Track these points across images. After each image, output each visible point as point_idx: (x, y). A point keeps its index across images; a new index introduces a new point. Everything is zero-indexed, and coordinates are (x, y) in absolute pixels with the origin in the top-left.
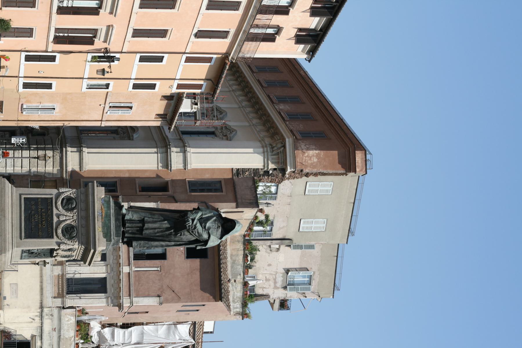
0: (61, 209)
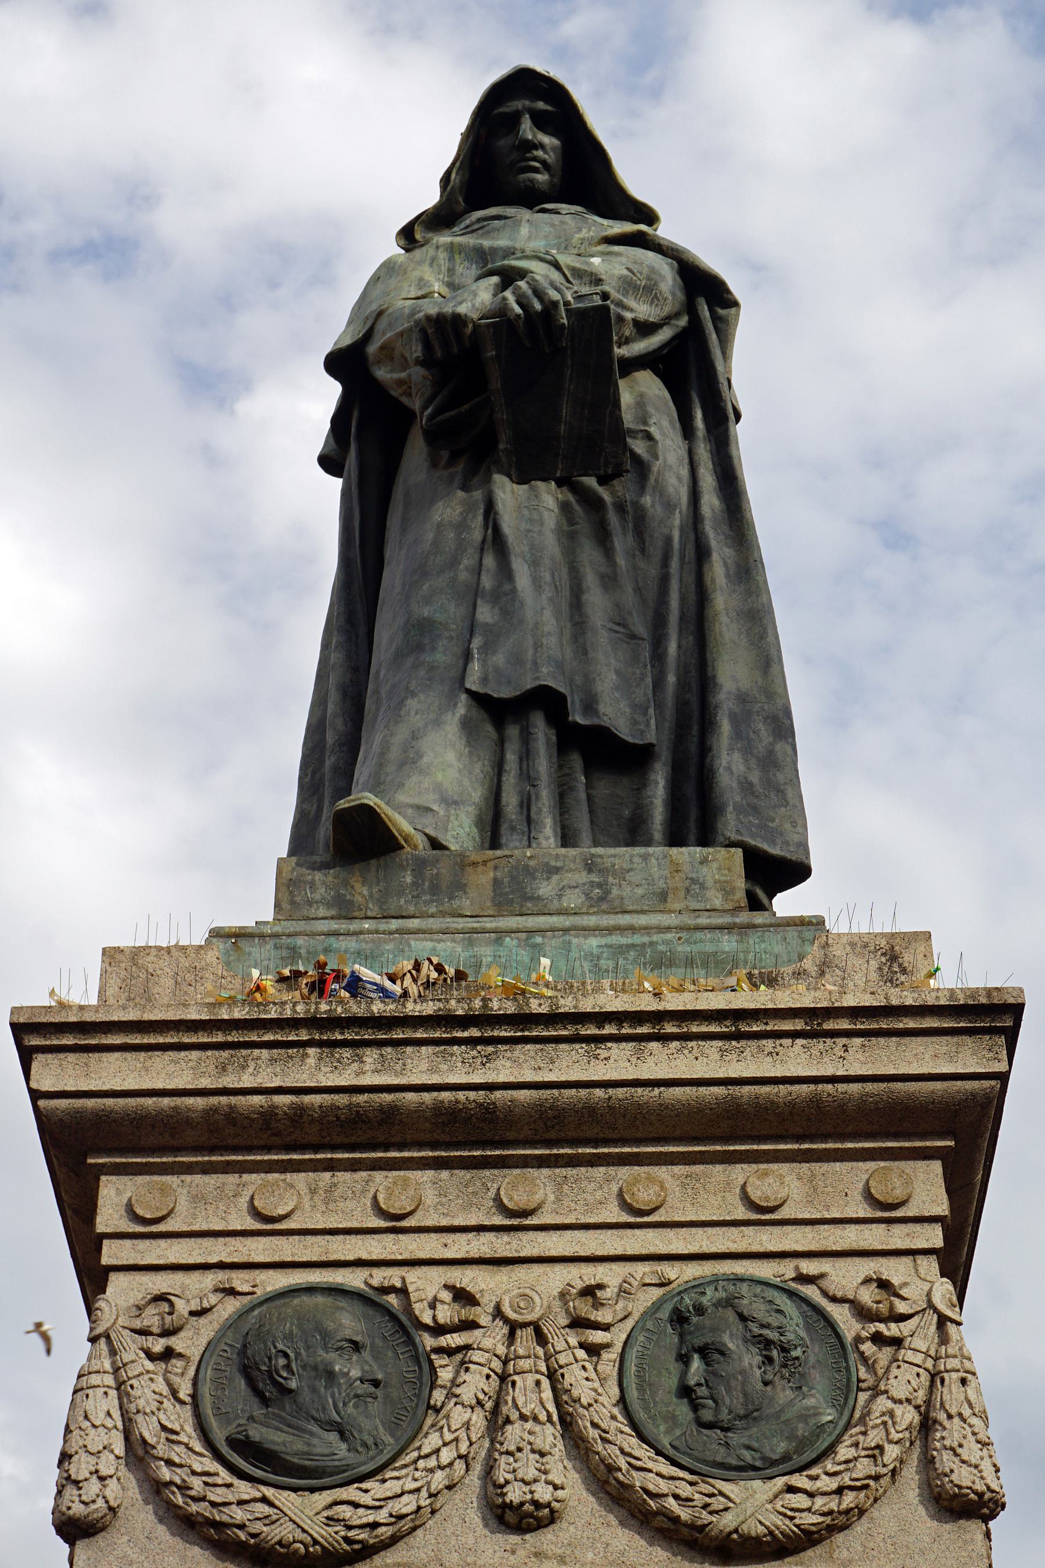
0: (393, 1487)
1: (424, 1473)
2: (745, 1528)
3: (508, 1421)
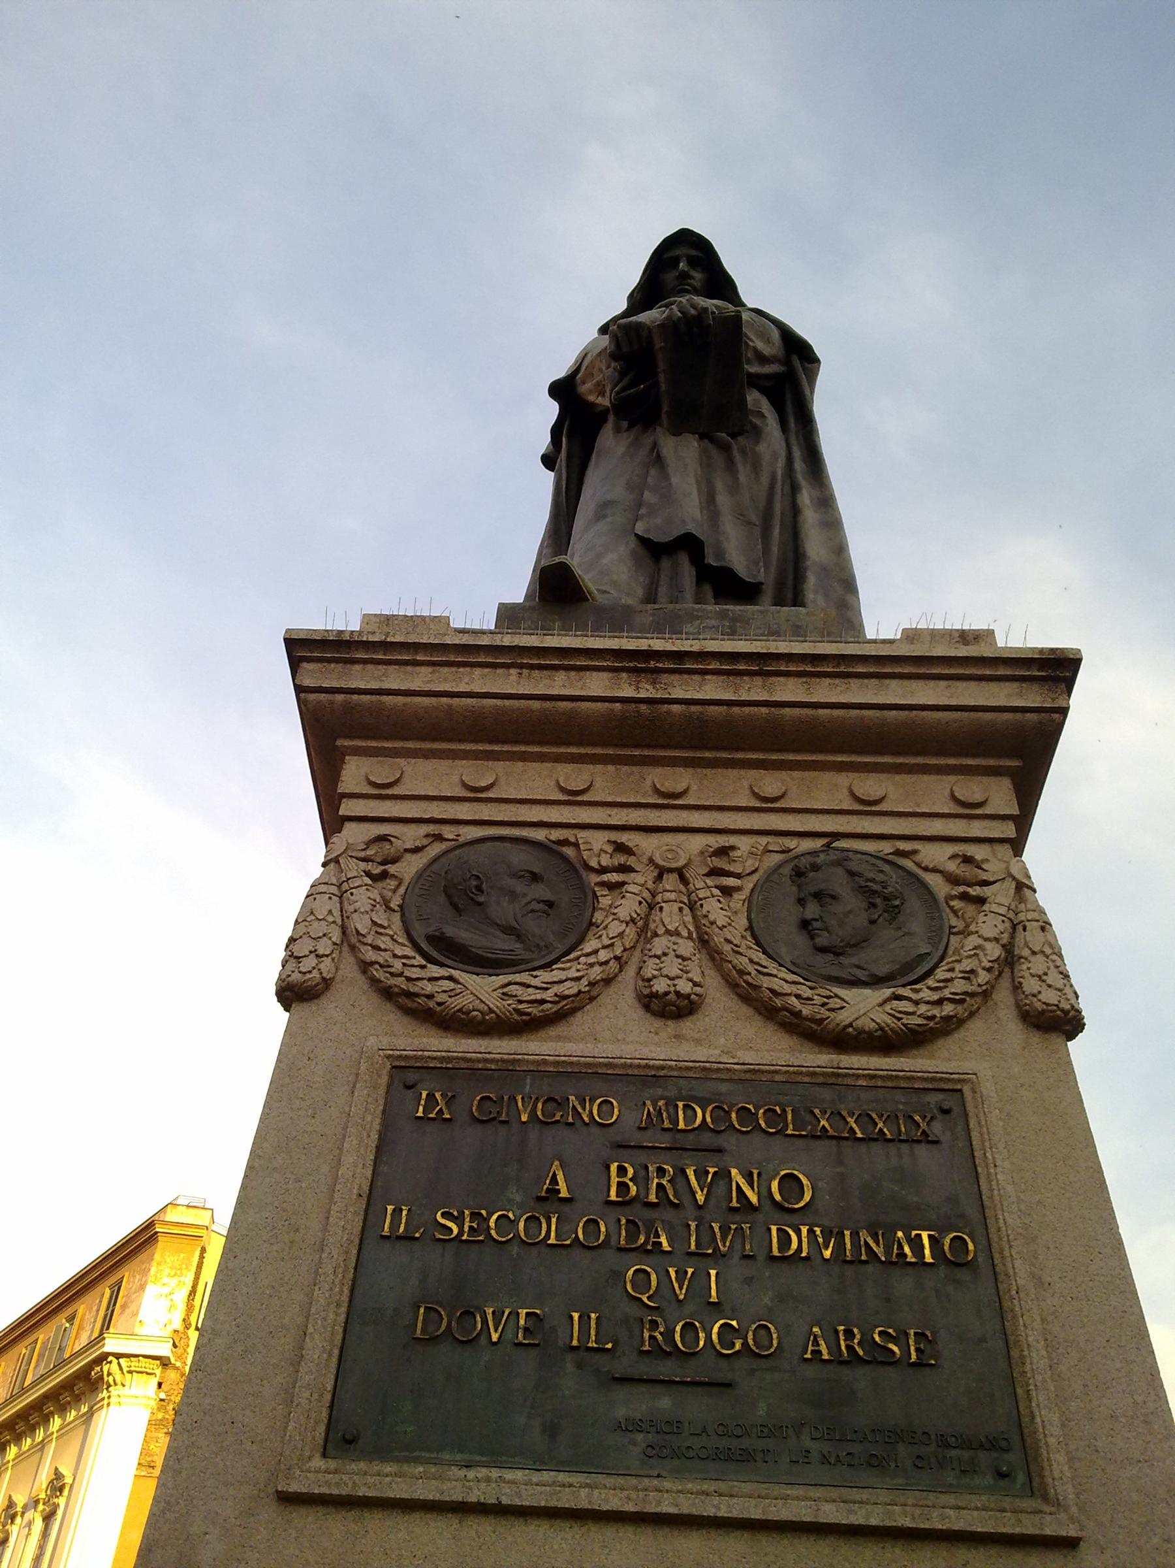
0: (556, 975)
1: (585, 967)
2: (859, 1023)
3: (656, 935)
